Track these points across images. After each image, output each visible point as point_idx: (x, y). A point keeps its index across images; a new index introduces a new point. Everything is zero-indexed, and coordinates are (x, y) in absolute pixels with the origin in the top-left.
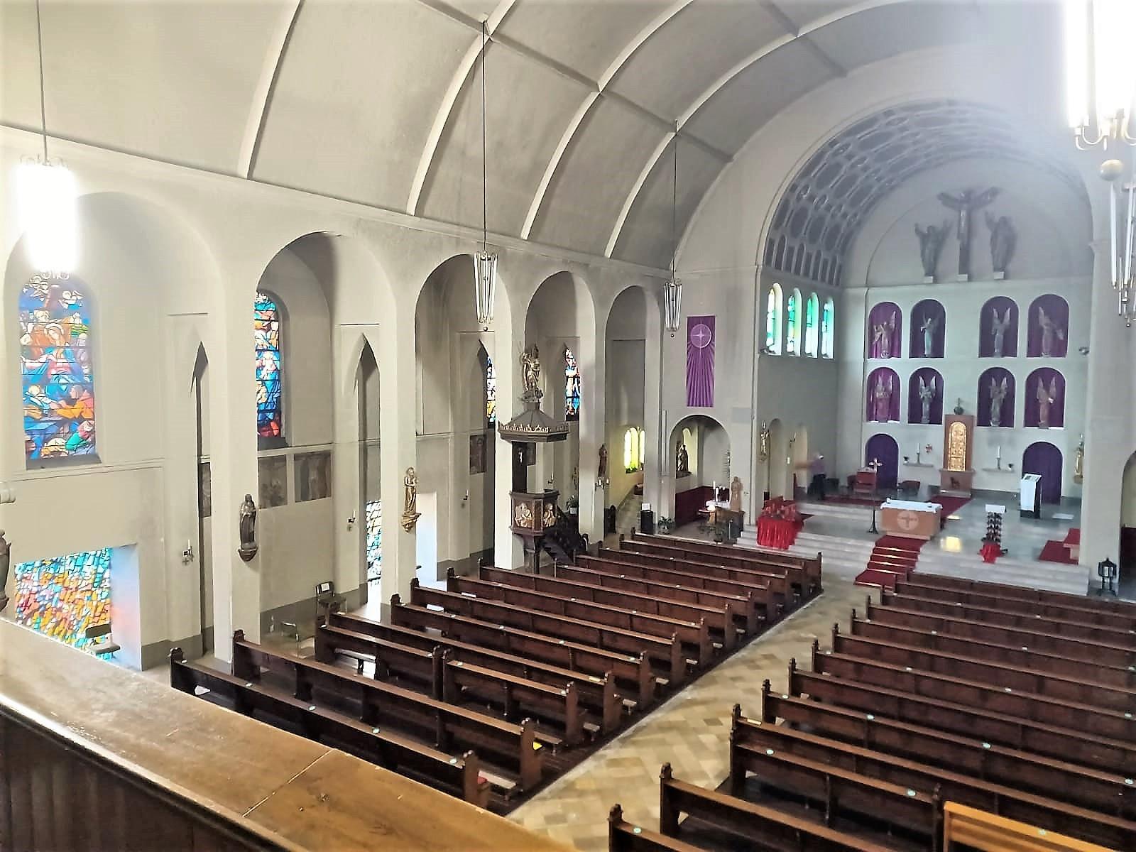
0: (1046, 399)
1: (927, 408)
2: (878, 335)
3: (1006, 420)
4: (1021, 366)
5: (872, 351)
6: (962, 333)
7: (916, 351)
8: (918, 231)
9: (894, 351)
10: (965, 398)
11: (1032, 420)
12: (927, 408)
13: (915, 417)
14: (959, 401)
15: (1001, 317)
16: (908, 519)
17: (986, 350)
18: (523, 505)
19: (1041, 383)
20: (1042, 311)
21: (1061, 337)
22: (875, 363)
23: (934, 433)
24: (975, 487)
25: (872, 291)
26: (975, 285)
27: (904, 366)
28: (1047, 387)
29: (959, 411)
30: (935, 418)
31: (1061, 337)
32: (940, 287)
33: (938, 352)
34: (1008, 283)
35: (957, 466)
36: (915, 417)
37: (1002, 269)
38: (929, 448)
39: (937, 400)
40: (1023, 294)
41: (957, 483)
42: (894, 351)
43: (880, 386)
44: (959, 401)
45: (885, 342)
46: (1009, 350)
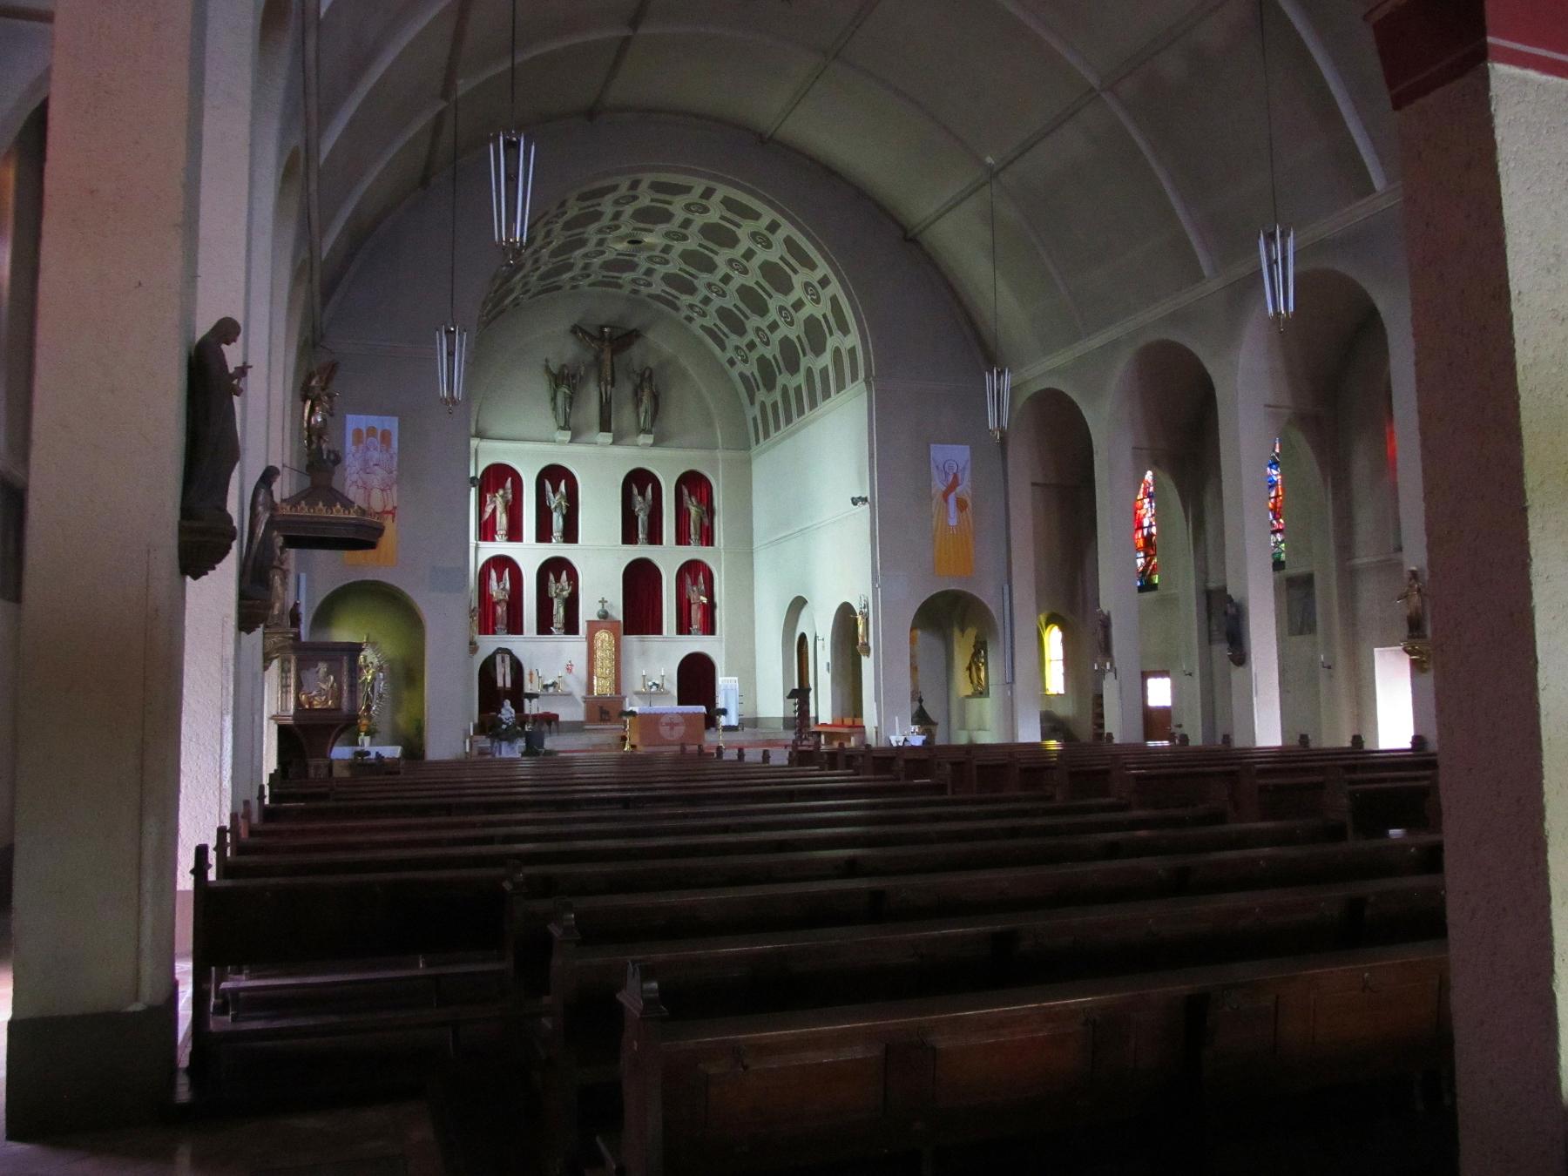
2: (489, 510)
4: (668, 558)
6: (600, 512)
7: (543, 535)
8: (547, 369)
9: (515, 534)
11: (683, 627)
12: (560, 613)
14: (603, 602)
16: (672, 725)
17: (629, 537)
18: (323, 668)
19: (689, 581)
20: (686, 492)
21: (706, 521)
23: (572, 649)
26: (617, 450)
27: (529, 555)
28: (695, 583)
29: (604, 615)
30: (571, 627)
31: (706, 521)
32: (577, 448)
33: (570, 535)
34: (657, 452)
35: (602, 686)
36: (544, 627)
37: (649, 432)
38: (569, 670)
39: (572, 604)
40: (667, 468)
41: (607, 713)
45: (502, 520)
46: (655, 537)
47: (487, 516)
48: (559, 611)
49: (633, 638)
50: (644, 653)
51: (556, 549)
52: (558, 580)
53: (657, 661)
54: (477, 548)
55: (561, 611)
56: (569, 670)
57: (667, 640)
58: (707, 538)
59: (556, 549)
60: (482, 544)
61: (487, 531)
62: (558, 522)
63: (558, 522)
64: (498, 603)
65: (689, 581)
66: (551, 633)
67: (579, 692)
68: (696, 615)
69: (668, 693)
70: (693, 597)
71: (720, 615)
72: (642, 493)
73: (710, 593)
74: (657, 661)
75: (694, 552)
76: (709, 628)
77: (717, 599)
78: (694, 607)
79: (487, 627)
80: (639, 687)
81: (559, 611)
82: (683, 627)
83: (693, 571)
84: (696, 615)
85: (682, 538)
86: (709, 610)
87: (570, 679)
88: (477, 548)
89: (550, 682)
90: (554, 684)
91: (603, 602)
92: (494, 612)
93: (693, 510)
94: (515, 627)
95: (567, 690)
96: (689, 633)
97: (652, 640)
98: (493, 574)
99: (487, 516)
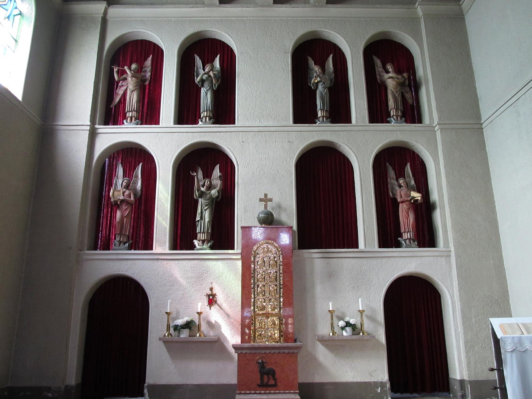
0: (405, 193)
1: (206, 207)
2: (121, 92)
3: (344, 236)
4: (360, 142)
5: (110, 112)
6: (263, 88)
7: (186, 114)
9: (149, 114)
10: (276, 196)
11: (389, 237)
13: (183, 238)
15: (322, 65)
17: (303, 113)
19: (391, 173)
20: (378, 63)
22: (110, 136)
24: (302, 379)
25: (115, 11)
27: (165, 141)
30: (222, 237)
33: (224, 113)
36: (183, 238)
38: (212, 300)
41: (272, 373)
42: (149, 114)
43: (120, 180)
44: (266, 200)
45: (133, 99)
46: (340, 113)
47: (117, 99)
48: (204, 216)
49: (314, 254)
50: (331, 275)
51: (204, 132)
52: (208, 175)
53: (354, 288)
54: (93, 135)
55: (207, 215)
56: (212, 300)
57: (367, 255)
58: (412, 114)
59: (204, 132)
60: (102, 129)
61: (110, 112)
62: (206, 98)
63: (206, 98)
64: (117, 205)
65: (391, 173)
66: (193, 247)
67: (232, 338)
68: (407, 219)
69: (372, 337)
70: (400, 194)
71: (443, 220)
72: (322, 65)
73: (422, 185)
74: (354, 288)
75: (394, 132)
76: (426, 237)
77: (435, 196)
78: (403, 208)
79: (101, 241)
80: (324, 330)
81: (204, 216)
82: (389, 237)
83: (396, 161)
84: (407, 219)
85: (378, 114)
86: (425, 211)
87: (214, 315)
88: (93, 135)
89: (180, 322)
90: (188, 325)
91: (266, 200)
92: (113, 217)
93: (391, 84)
94: (142, 240)
95: (212, 334)
96: (398, 245)
97: (343, 259)
98: (120, 171)
99: (117, 99)
